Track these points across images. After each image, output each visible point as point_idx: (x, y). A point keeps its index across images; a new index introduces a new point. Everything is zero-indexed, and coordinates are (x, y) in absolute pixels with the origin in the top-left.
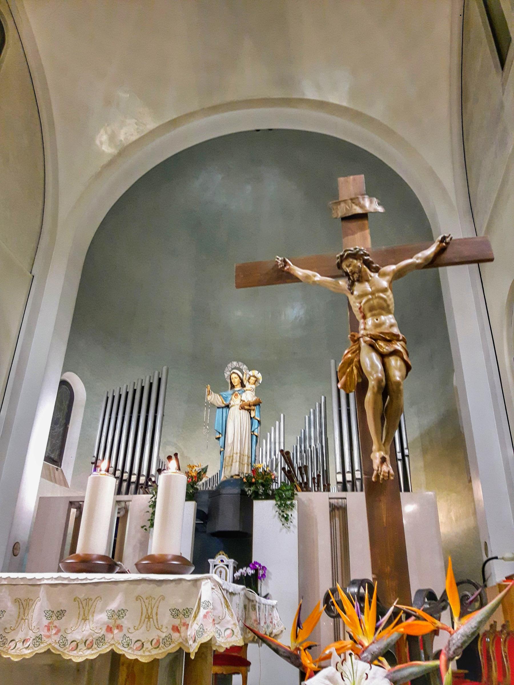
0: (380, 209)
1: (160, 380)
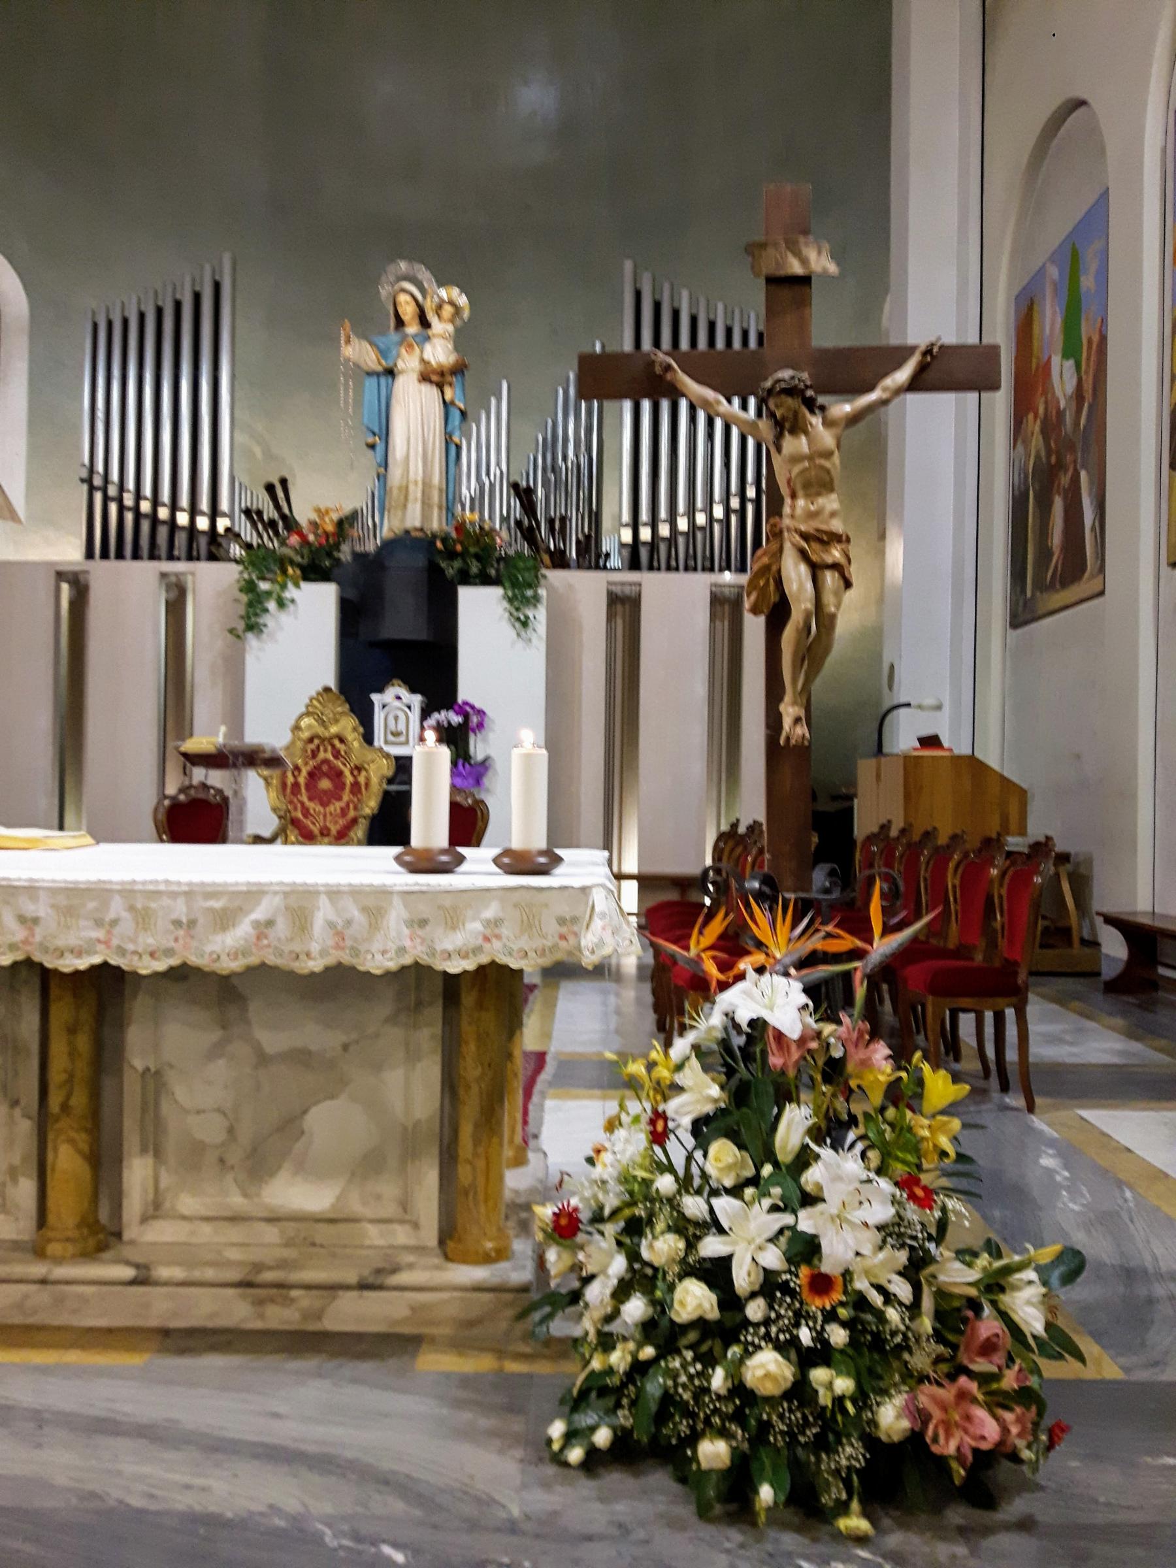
0: (832, 268)
1: (217, 287)
